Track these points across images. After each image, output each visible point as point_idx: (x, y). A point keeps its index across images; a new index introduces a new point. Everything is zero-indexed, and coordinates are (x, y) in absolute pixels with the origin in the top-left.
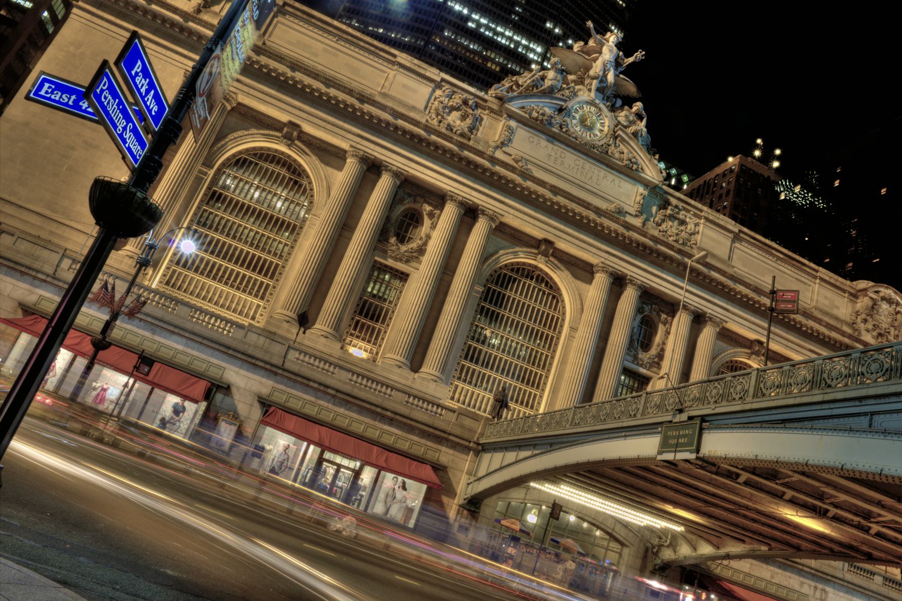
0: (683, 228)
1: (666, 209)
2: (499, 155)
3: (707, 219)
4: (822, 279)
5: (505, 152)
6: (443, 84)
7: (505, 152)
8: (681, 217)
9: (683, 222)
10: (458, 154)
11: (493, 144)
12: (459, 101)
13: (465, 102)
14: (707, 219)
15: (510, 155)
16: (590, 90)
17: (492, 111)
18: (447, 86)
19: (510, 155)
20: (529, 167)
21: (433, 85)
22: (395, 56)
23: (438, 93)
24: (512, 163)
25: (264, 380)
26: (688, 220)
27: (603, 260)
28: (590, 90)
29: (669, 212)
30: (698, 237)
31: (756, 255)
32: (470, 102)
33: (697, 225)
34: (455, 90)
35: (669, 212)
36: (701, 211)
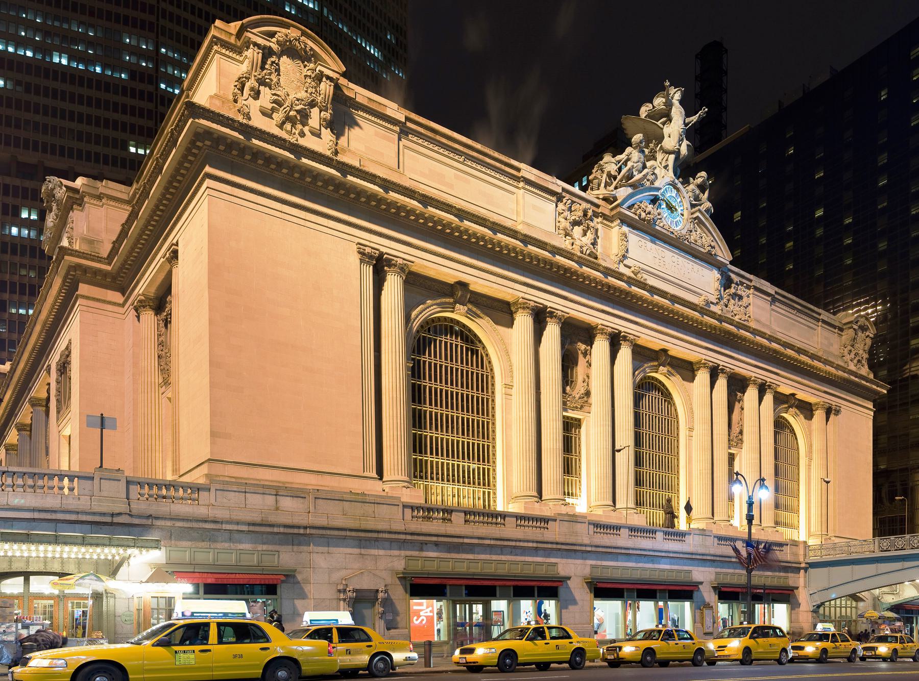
0: (740, 303)
1: (730, 287)
2: (622, 269)
3: (756, 289)
4: (824, 322)
5: (625, 266)
6: (564, 194)
7: (625, 266)
8: (739, 292)
9: (741, 298)
10: (601, 282)
11: (617, 259)
12: (581, 214)
13: (585, 215)
14: (756, 289)
15: (630, 267)
16: (666, 167)
17: (605, 217)
18: (568, 196)
19: (630, 267)
20: (645, 276)
21: (554, 199)
22: (518, 170)
23: (561, 206)
24: (632, 275)
25: (707, 569)
26: (743, 294)
27: (704, 357)
28: (666, 167)
29: (732, 290)
30: (751, 307)
31: (783, 312)
32: (590, 213)
33: (748, 297)
34: (575, 199)
35: (732, 290)
36: (751, 281)
